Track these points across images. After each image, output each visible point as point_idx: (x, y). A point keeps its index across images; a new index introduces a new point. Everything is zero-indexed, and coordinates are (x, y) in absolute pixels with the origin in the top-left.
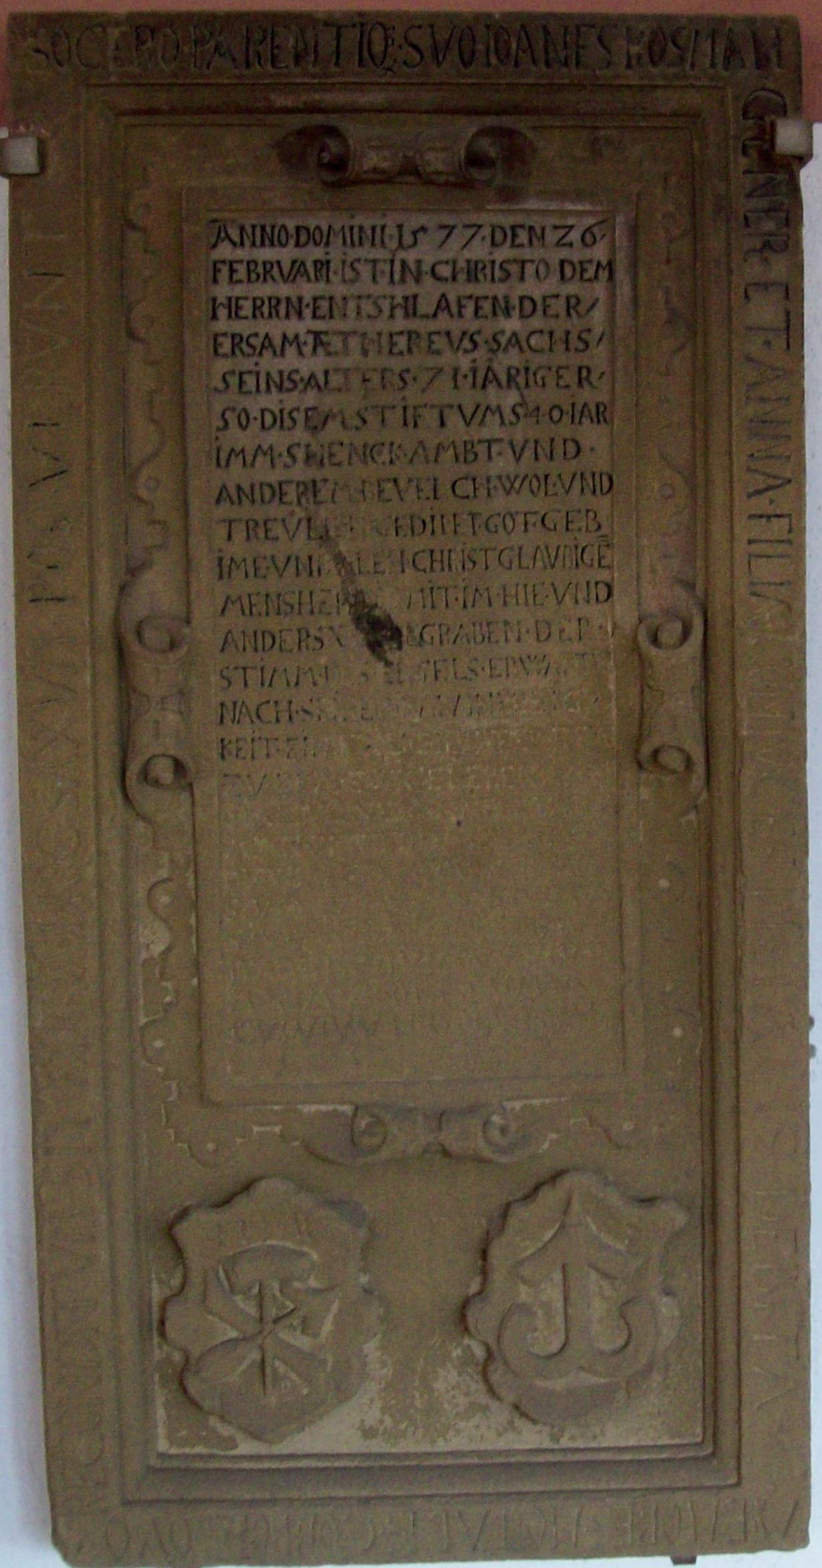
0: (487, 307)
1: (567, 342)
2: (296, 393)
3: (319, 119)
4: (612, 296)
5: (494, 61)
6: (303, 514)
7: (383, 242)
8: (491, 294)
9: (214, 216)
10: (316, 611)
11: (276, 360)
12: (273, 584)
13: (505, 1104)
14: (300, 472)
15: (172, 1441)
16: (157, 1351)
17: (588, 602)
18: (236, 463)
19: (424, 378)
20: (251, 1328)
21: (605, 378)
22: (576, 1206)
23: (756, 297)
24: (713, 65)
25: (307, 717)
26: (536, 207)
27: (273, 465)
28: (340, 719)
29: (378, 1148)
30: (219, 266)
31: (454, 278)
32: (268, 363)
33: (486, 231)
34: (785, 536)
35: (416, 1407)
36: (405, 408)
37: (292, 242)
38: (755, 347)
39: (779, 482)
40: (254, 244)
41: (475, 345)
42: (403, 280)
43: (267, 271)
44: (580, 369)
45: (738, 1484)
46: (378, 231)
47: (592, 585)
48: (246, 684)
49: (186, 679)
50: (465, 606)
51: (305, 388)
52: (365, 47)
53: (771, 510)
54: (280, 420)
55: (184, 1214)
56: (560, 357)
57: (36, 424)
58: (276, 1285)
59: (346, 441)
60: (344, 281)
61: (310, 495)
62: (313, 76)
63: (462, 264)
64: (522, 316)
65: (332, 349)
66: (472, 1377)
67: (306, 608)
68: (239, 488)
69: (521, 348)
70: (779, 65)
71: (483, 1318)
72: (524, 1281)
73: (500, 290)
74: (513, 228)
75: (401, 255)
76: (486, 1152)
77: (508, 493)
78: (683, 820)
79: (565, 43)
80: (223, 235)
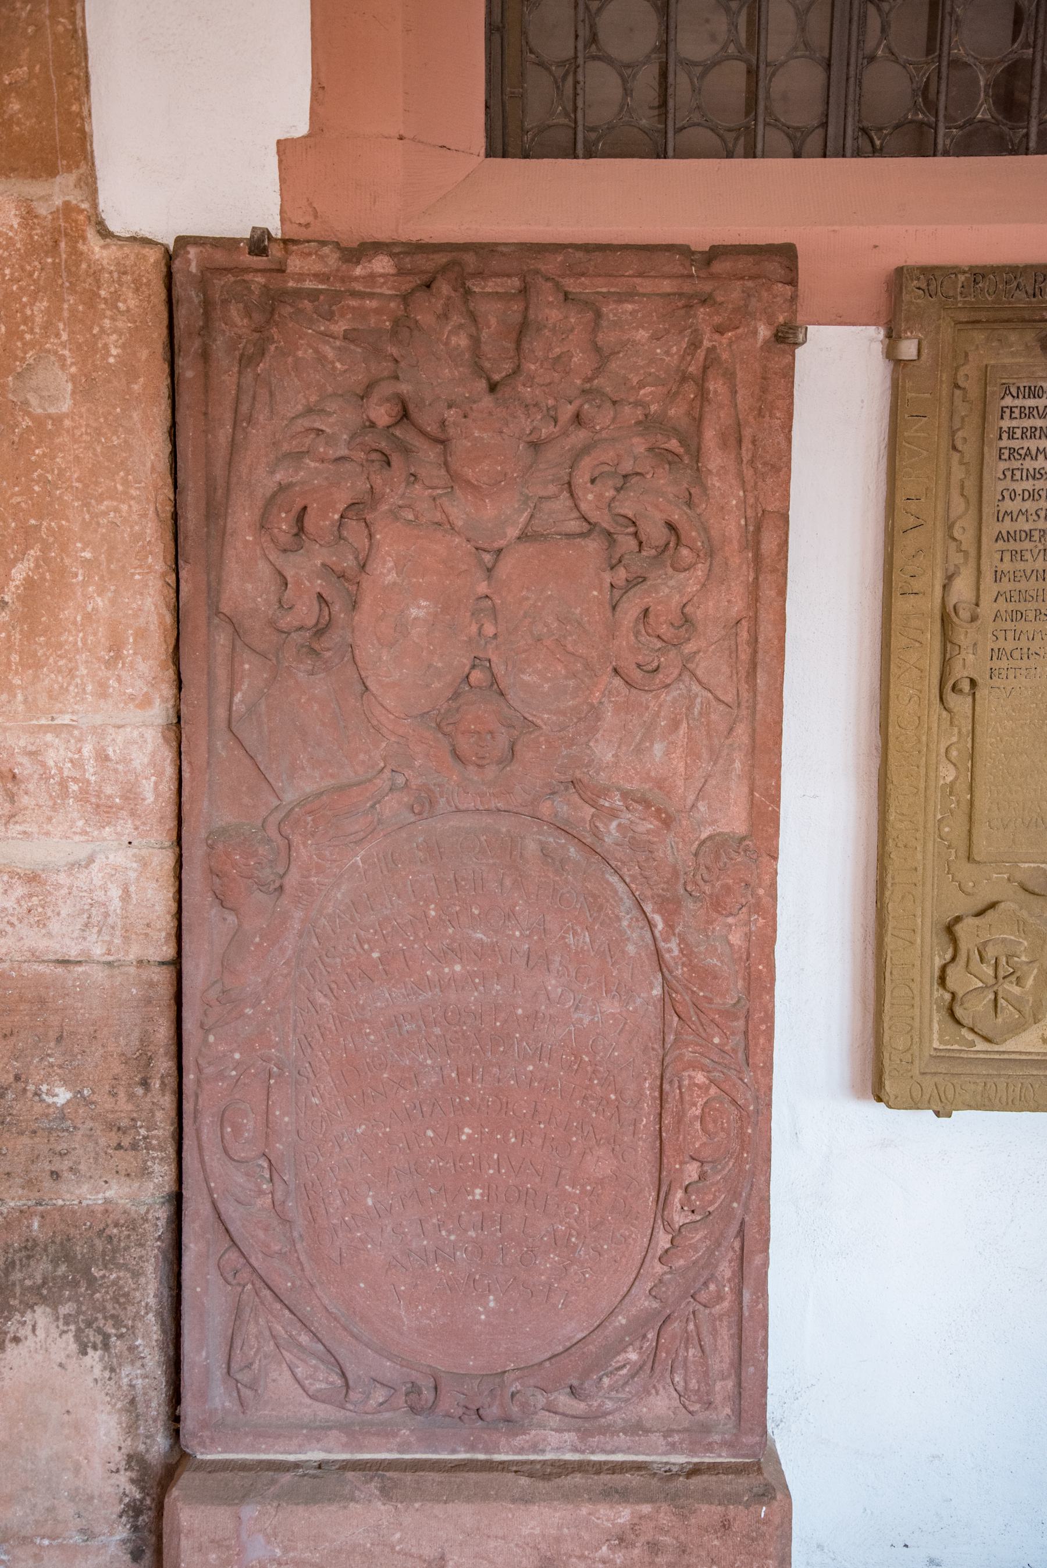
9: (1004, 381)
12: (1023, 585)
18: (1008, 519)
20: (992, 981)
32: (1029, 464)
55: (958, 919)
67: (1040, 598)
68: (1008, 532)
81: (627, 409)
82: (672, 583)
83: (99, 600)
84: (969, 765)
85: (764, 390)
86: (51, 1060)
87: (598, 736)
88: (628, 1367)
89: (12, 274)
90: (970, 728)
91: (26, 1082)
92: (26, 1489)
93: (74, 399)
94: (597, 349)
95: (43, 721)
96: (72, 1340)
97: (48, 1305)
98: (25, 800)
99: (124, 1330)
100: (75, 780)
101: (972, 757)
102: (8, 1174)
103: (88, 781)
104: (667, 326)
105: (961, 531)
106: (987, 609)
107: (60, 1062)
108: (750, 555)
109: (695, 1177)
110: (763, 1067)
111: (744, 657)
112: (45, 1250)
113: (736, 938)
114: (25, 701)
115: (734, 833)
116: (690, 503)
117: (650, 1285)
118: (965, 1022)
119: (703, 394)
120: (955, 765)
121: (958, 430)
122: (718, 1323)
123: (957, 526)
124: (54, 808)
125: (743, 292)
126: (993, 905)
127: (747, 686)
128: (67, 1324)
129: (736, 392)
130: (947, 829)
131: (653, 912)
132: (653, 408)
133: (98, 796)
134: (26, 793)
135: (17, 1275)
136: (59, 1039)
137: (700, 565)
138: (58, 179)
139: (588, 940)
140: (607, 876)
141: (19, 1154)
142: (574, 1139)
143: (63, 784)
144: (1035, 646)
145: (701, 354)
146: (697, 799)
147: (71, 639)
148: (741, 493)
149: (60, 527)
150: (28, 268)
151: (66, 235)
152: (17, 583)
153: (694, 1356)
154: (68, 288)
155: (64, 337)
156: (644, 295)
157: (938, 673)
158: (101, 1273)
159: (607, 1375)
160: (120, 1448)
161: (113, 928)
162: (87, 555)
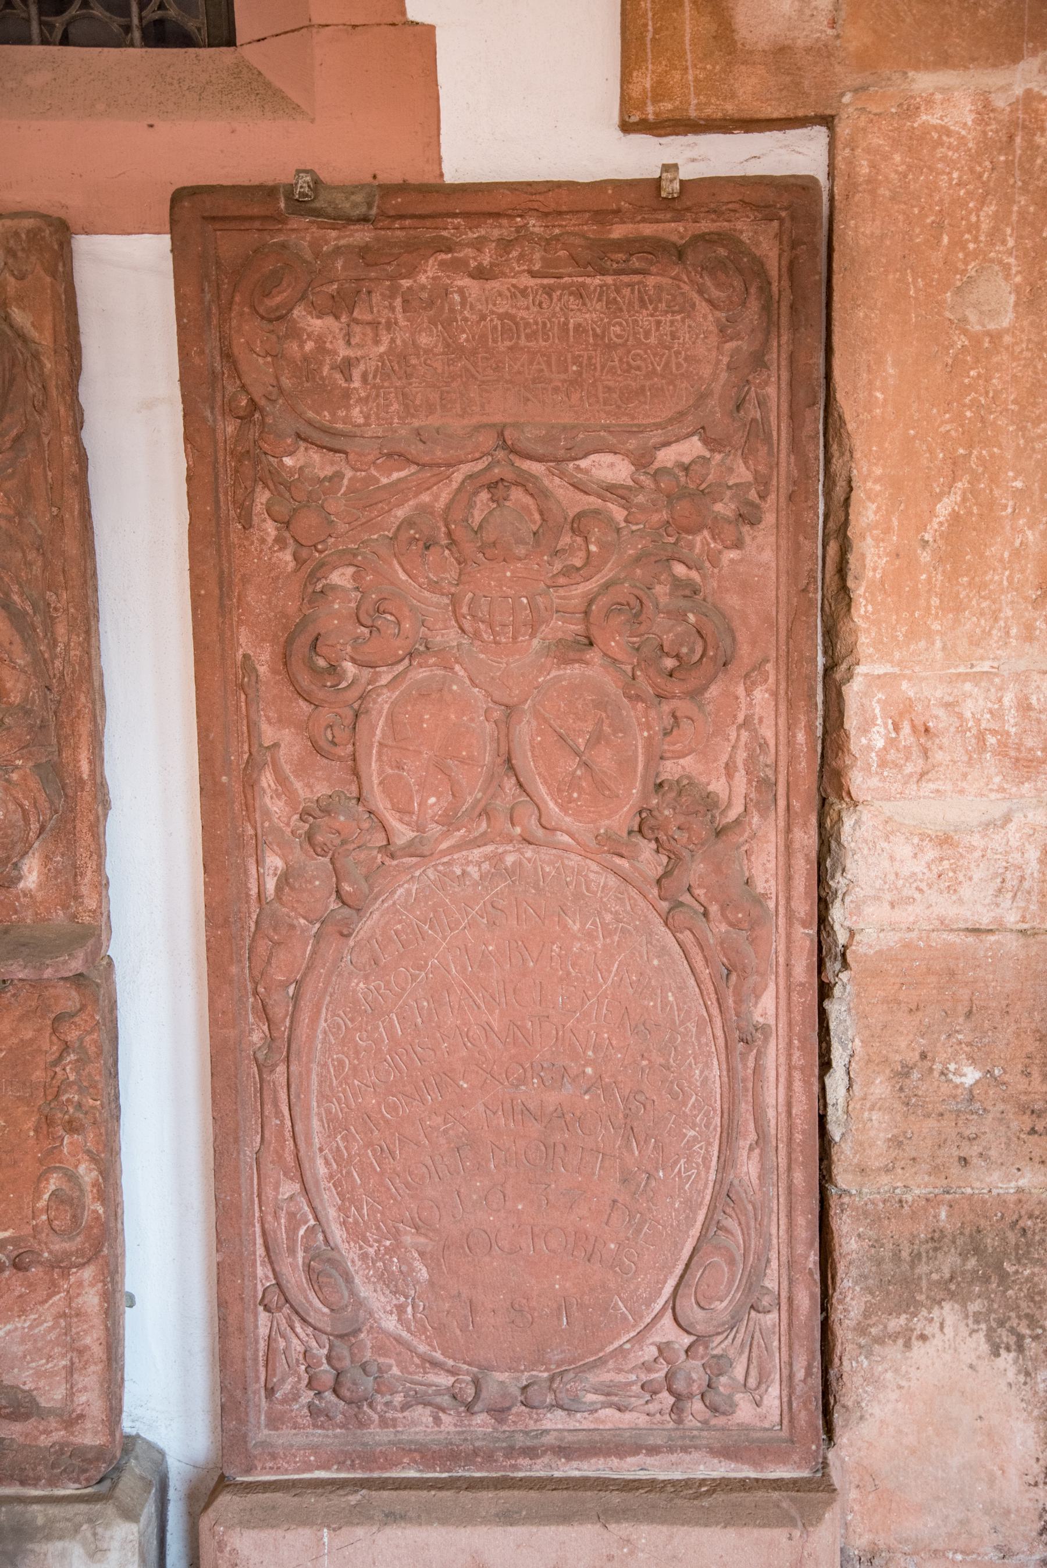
83: (1029, 533)
86: (960, 1037)
89: (960, 178)
91: (933, 1061)
92: (938, 1498)
93: (1017, 312)
95: (962, 669)
96: (983, 1340)
97: (956, 1302)
98: (939, 756)
99: (1040, 1331)
100: (994, 732)
102: (914, 1159)
103: (1008, 733)
107: (968, 1039)
112: (954, 1242)
114: (944, 648)
124: (970, 762)
128: (977, 1322)
133: (1019, 750)
134: (941, 748)
135: (922, 1269)
136: (969, 1014)
138: (1022, 65)
141: (925, 1138)
143: (981, 737)
147: (996, 578)
149: (992, 456)
150: (978, 169)
151: (1024, 127)
152: (942, 519)
154: (1020, 188)
155: (1011, 243)
158: (1014, 1268)
160: (1038, 1460)
161: (1029, 893)
162: (1019, 484)
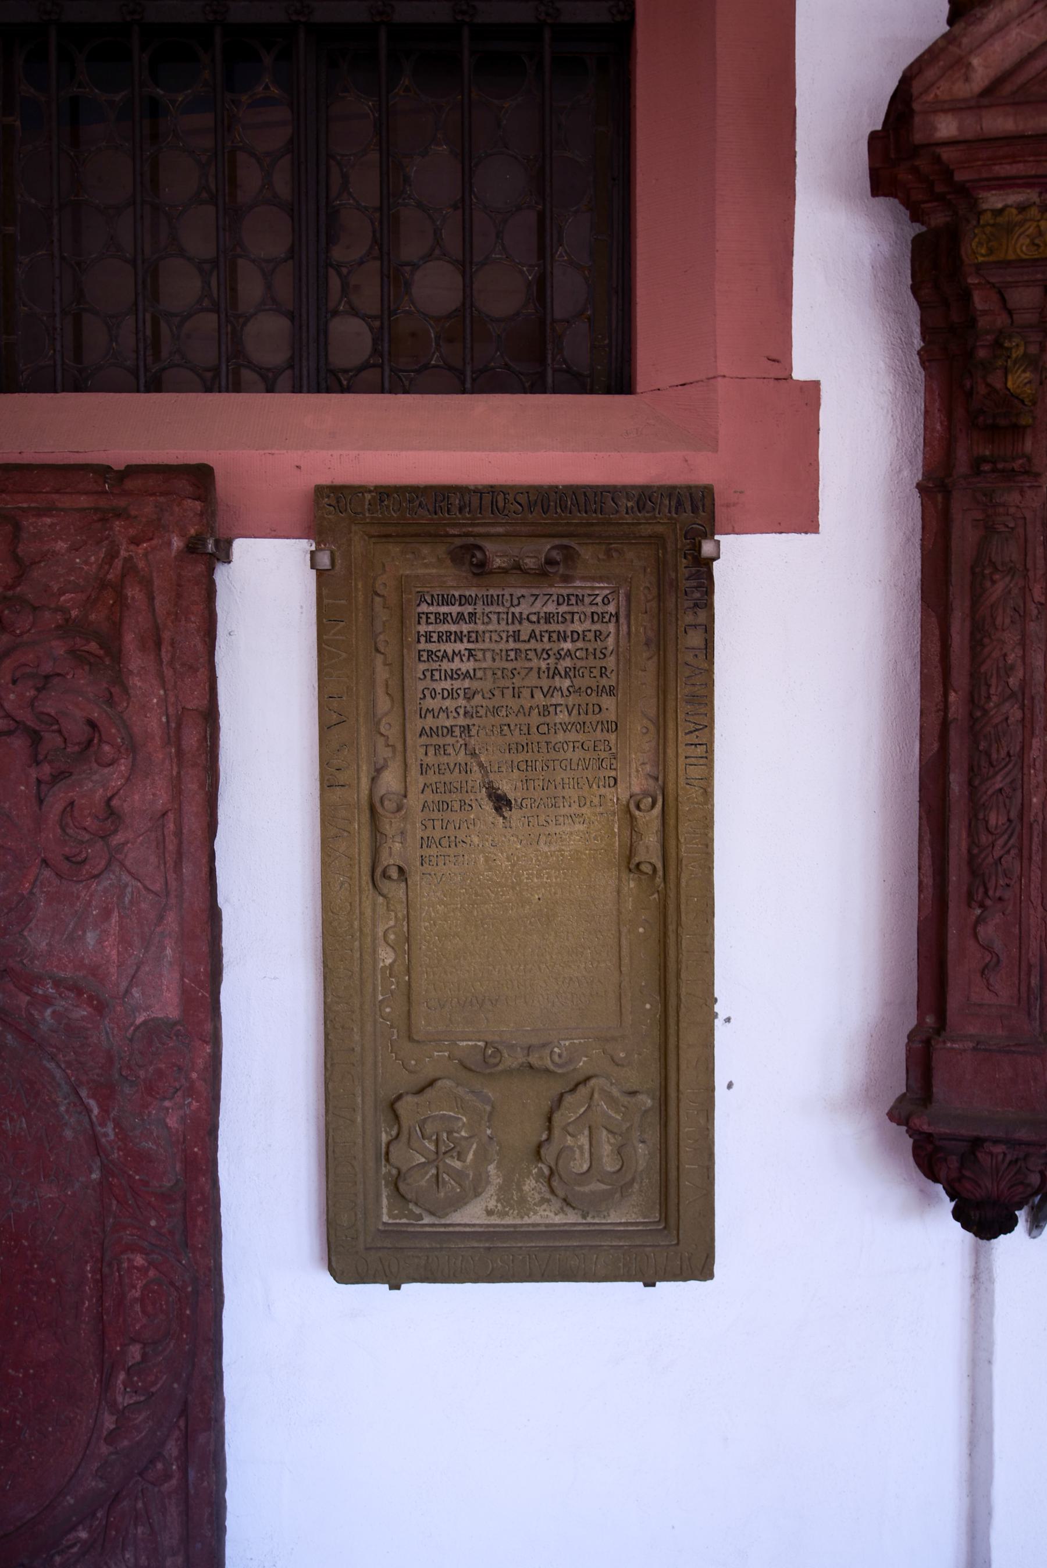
0: (555, 636)
1: (595, 654)
2: (459, 680)
3: (471, 540)
4: (618, 630)
5: (559, 510)
6: (463, 742)
7: (503, 603)
8: (557, 630)
9: (419, 589)
10: (469, 791)
11: (449, 664)
12: (447, 777)
13: (561, 1042)
14: (462, 721)
15: (390, 1216)
16: (383, 1168)
17: (605, 787)
18: (430, 716)
19: (523, 672)
20: (433, 1157)
21: (613, 672)
22: (596, 1096)
23: (691, 632)
24: (670, 512)
25: (464, 845)
26: (580, 585)
27: (448, 717)
28: (481, 846)
29: (497, 1065)
30: (421, 615)
31: (539, 622)
32: (445, 665)
33: (555, 598)
34: (704, 755)
35: (513, 1199)
36: (514, 688)
37: (457, 603)
38: (689, 658)
39: (701, 727)
40: (438, 604)
41: (549, 655)
42: (513, 623)
43: (444, 618)
44: (601, 668)
45: (678, 1244)
46: (500, 597)
47: (607, 778)
48: (434, 828)
49: (405, 826)
50: (543, 789)
51: (464, 678)
52: (494, 503)
53: (697, 741)
54: (452, 694)
55: (399, 1097)
56: (591, 662)
57: (330, 697)
58: (445, 1135)
59: (484, 705)
60: (483, 623)
61: (466, 732)
62: (468, 519)
63: (542, 614)
64: (573, 641)
65: (477, 658)
66: (542, 1184)
68: (431, 728)
69: (572, 658)
70: (704, 512)
71: (549, 1153)
72: (570, 1134)
73: (561, 628)
74: (568, 595)
75: (512, 609)
76: (552, 1067)
77: (565, 732)
78: (651, 898)
79: (595, 500)
80: (423, 600)
81: (47, 614)
82: (95, 777)
84: (406, 948)
85: (179, 596)
87: (32, 925)
88: (79, 1545)
90: (405, 913)
94: (17, 559)
101: (408, 940)
104: (84, 538)
105: (387, 727)
106: (414, 801)
108: (173, 750)
109: (138, 1357)
110: (201, 1249)
111: (171, 847)
113: (172, 1122)
115: (168, 1018)
116: (110, 700)
117: (96, 1465)
118: (409, 1197)
119: (121, 600)
120: (393, 948)
121: (380, 633)
122: (166, 1500)
123: (383, 722)
125: (156, 507)
126: (431, 1083)
127: (174, 876)
129: (153, 599)
130: (388, 1010)
131: (89, 1097)
132: (74, 613)
137: (123, 761)
139: (25, 1126)
140: (45, 1062)
142: (16, 1323)
144: (461, 835)
145: (118, 563)
146: (131, 985)
148: (162, 692)
153: (143, 1533)
156: (62, 510)
157: (369, 861)
159: (58, 1553)
